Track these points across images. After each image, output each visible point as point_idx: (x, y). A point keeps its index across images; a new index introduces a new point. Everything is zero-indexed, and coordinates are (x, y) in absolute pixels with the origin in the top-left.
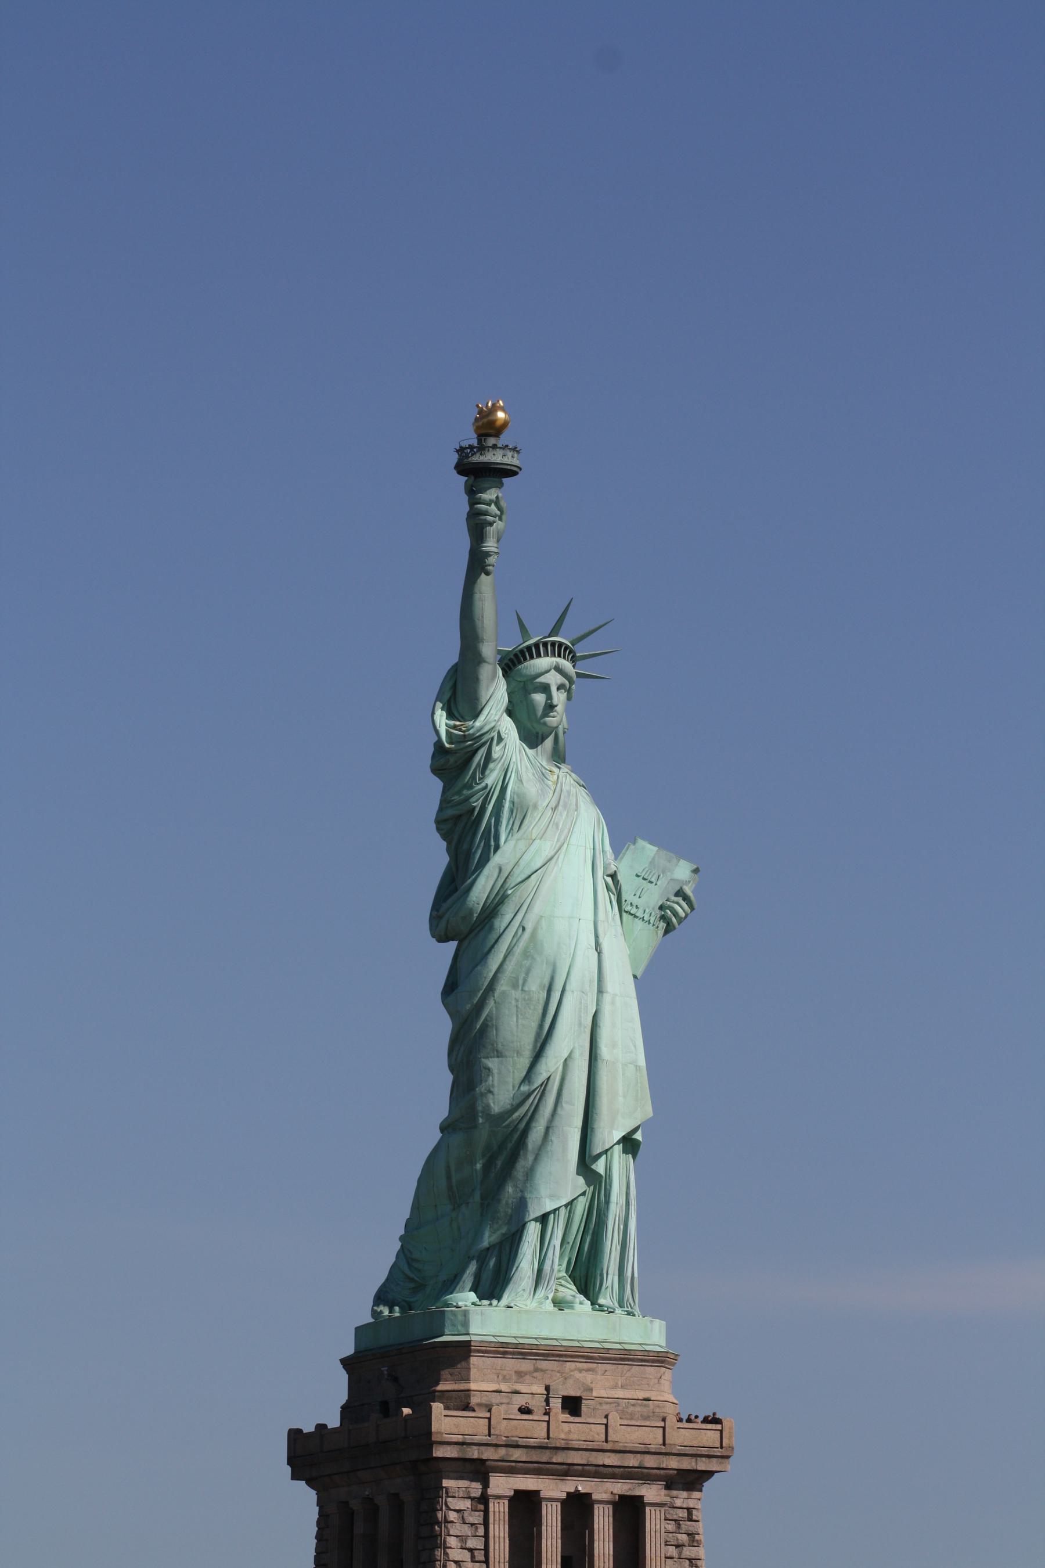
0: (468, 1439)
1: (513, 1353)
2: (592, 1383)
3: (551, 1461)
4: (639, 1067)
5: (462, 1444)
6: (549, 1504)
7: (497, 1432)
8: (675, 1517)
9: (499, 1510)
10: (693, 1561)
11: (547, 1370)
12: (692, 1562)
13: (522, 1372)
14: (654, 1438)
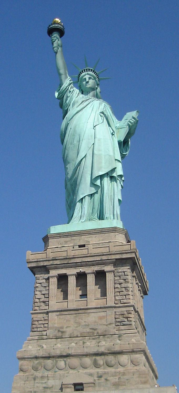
0: (39, 260)
1: (63, 236)
2: (91, 241)
3: (68, 263)
4: (110, 155)
5: (37, 261)
6: (71, 276)
7: (48, 257)
8: (118, 275)
9: (54, 281)
10: (126, 288)
11: (75, 239)
12: (125, 289)
13: (67, 241)
14: (106, 250)
